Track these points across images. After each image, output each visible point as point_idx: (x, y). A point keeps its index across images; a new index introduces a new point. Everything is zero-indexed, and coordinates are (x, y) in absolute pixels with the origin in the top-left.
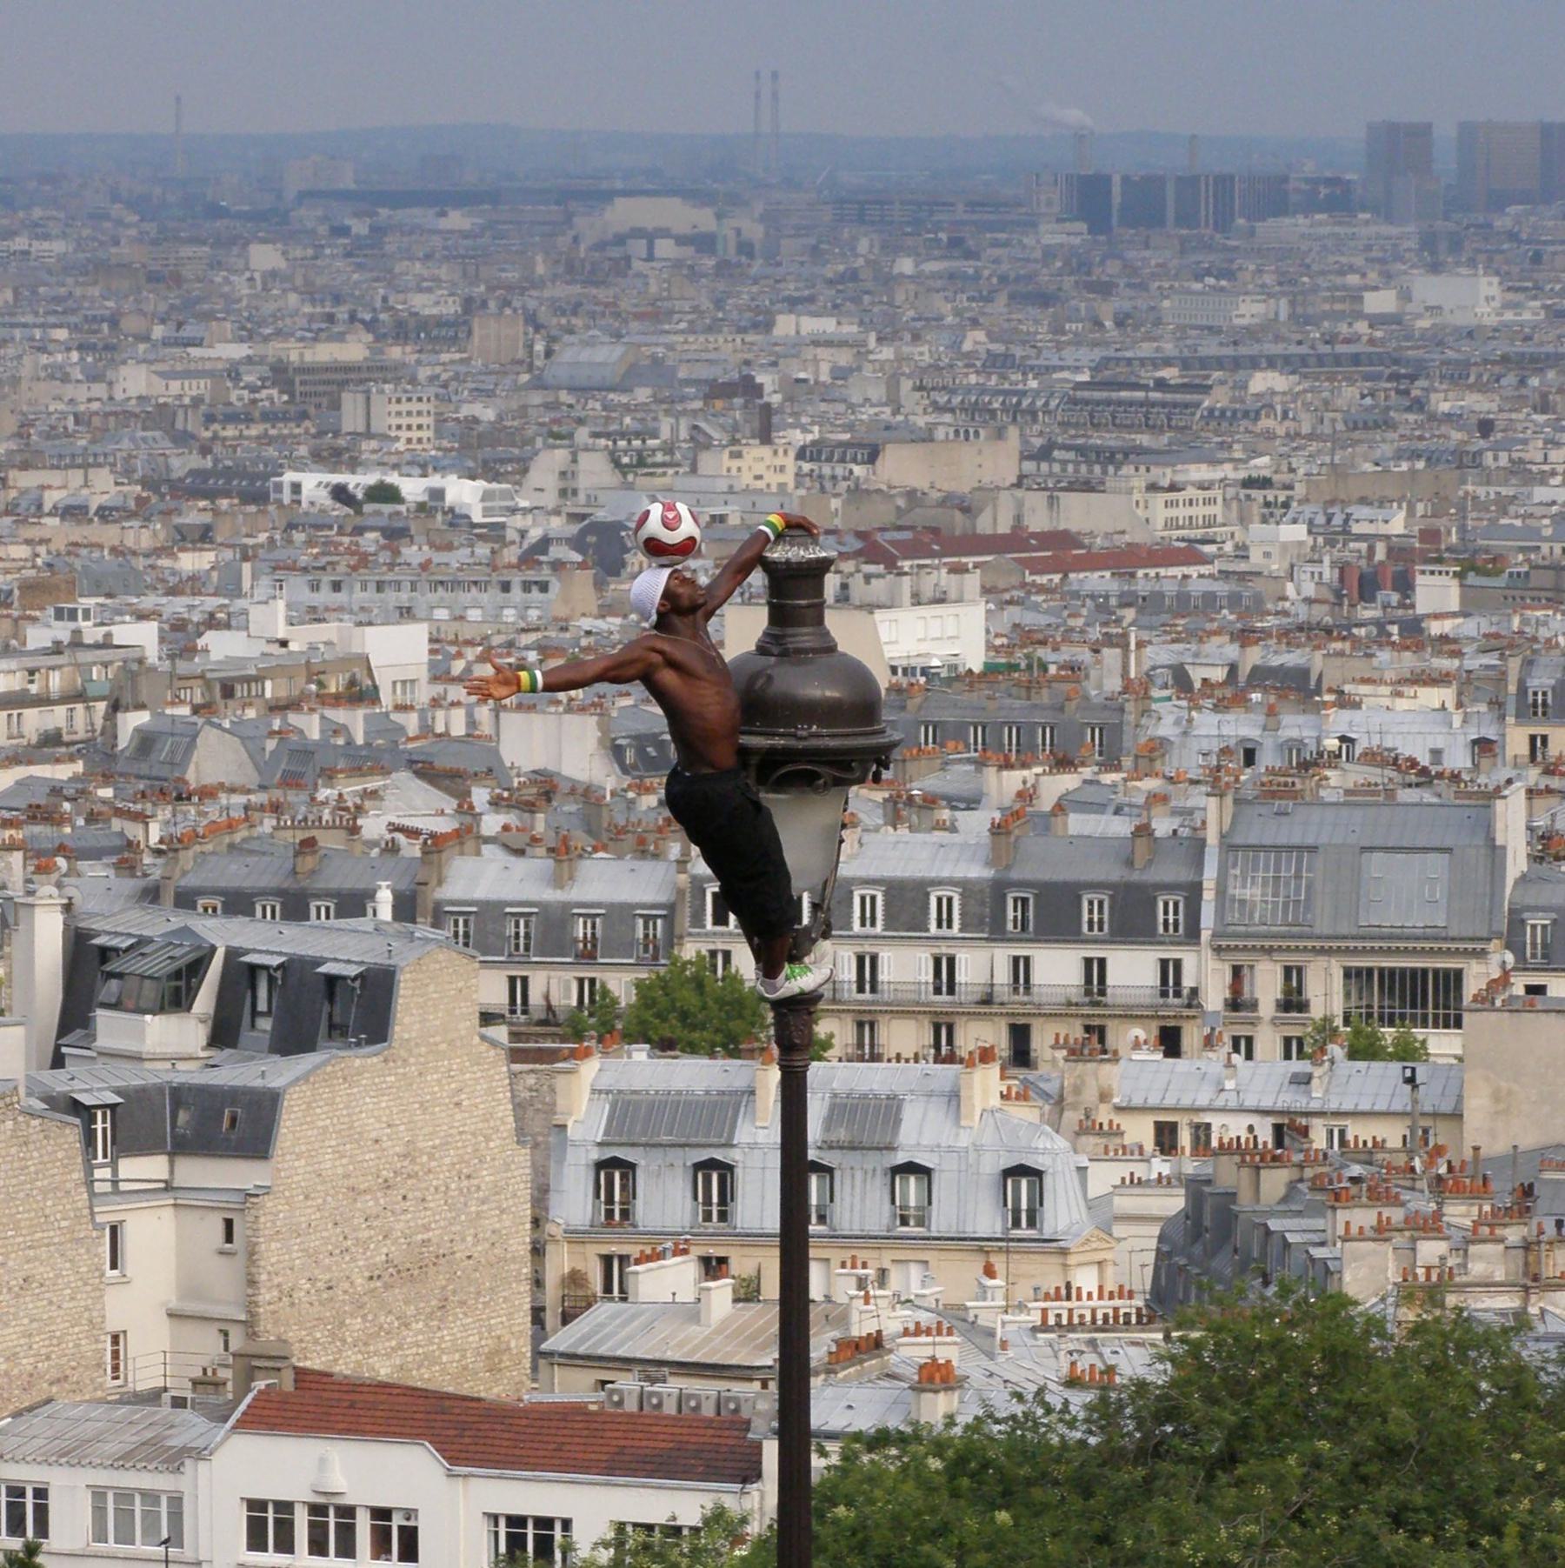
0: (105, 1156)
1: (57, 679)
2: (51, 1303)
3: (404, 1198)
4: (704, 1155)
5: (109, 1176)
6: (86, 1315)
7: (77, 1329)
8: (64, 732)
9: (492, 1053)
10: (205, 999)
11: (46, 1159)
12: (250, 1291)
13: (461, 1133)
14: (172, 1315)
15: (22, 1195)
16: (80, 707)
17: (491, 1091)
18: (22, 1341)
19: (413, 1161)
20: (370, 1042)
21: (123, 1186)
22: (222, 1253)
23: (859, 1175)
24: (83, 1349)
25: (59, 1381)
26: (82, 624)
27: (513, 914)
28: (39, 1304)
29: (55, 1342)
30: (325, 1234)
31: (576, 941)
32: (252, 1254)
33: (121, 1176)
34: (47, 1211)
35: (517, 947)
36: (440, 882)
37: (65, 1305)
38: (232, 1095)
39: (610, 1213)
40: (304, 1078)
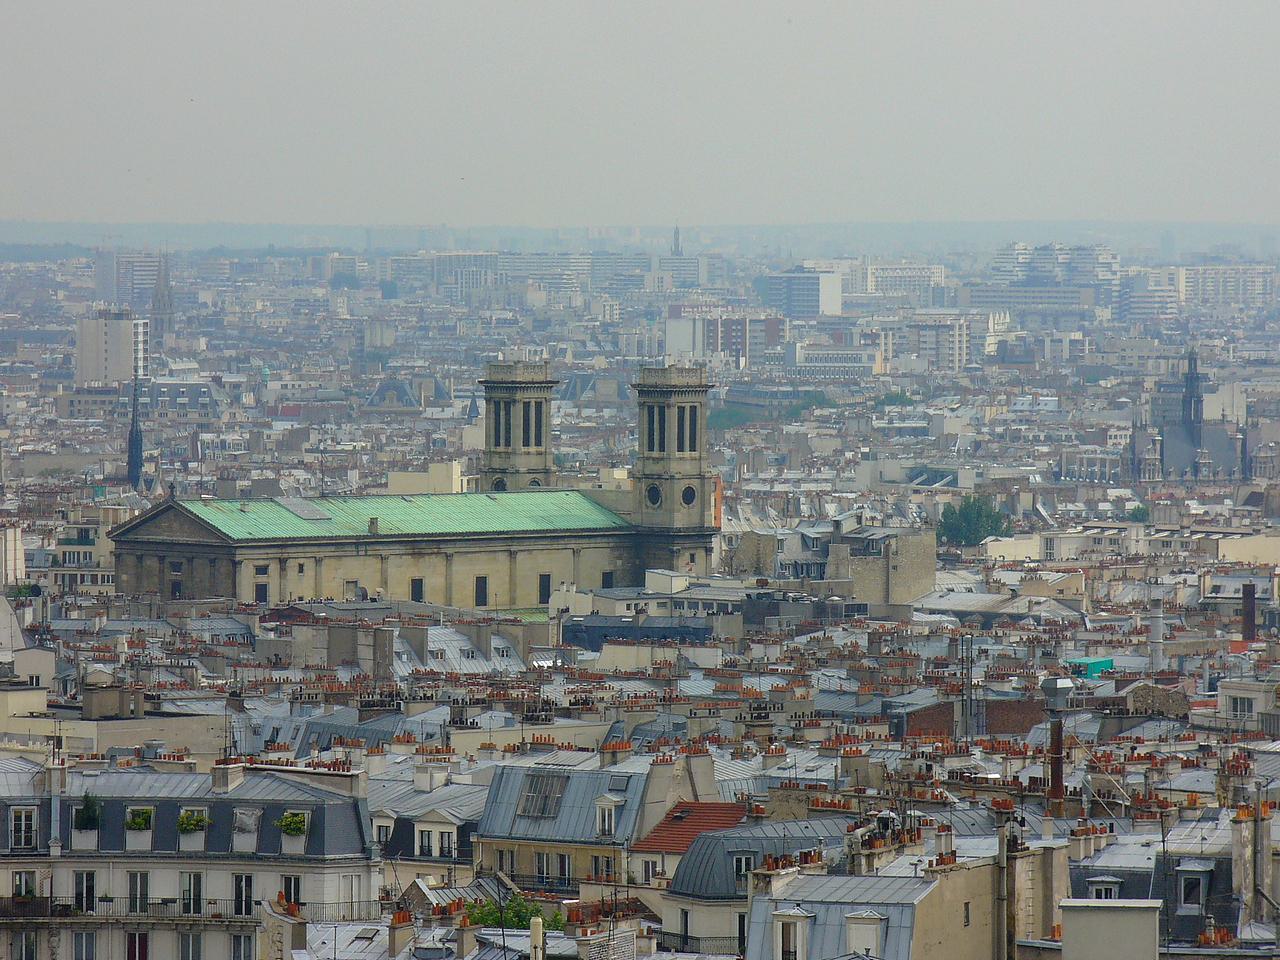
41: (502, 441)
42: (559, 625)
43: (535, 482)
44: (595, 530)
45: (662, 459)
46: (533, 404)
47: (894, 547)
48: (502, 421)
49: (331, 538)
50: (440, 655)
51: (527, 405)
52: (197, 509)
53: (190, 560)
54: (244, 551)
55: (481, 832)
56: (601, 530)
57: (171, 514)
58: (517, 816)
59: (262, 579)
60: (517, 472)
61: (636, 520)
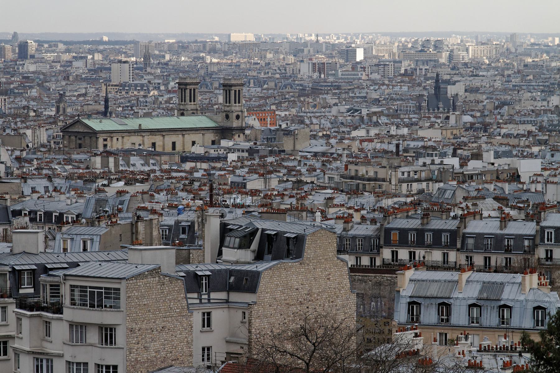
0: (206, 291)
1: (424, 175)
2: (172, 335)
3: (308, 307)
4: (441, 301)
5: (207, 298)
6: (186, 339)
7: (182, 344)
8: (425, 190)
9: (342, 263)
10: (255, 245)
11: (171, 290)
12: (249, 335)
13: (329, 288)
14: (227, 342)
15: (162, 301)
16: (430, 182)
17: (341, 275)
18: (161, 347)
19: (311, 296)
20: (296, 258)
21: (212, 301)
22: (242, 322)
23: (489, 308)
24: (184, 350)
25: (175, 360)
26: (435, 158)
27: (486, 238)
28: (168, 335)
29: (174, 347)
30: (277, 318)
31: (505, 246)
32: (250, 323)
33: (211, 298)
34: (171, 306)
35: (488, 247)
36: (465, 228)
37: (178, 336)
38: (247, 272)
39: (413, 319)
40: (270, 268)
41: (183, 101)
42: (179, 156)
43: (193, 113)
44: (209, 127)
45: (230, 106)
46: (192, 89)
47: (296, 133)
48: (183, 95)
49: (127, 130)
50: (134, 165)
51: (190, 90)
52: (86, 121)
53: (84, 137)
54: (100, 134)
55: (83, 216)
56: (211, 127)
57: (78, 123)
58: (93, 212)
59: (105, 143)
60: (188, 110)
61: (222, 124)
